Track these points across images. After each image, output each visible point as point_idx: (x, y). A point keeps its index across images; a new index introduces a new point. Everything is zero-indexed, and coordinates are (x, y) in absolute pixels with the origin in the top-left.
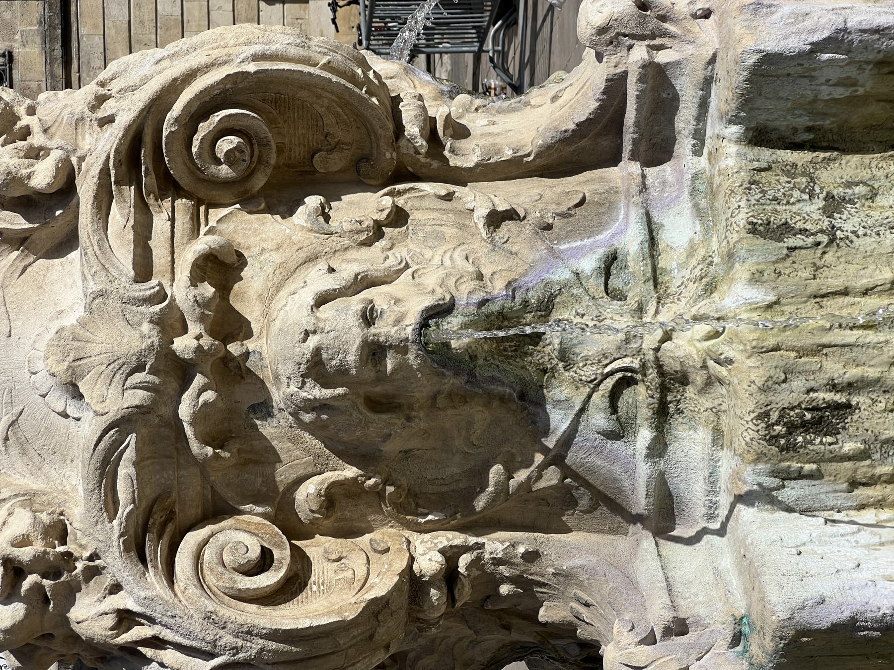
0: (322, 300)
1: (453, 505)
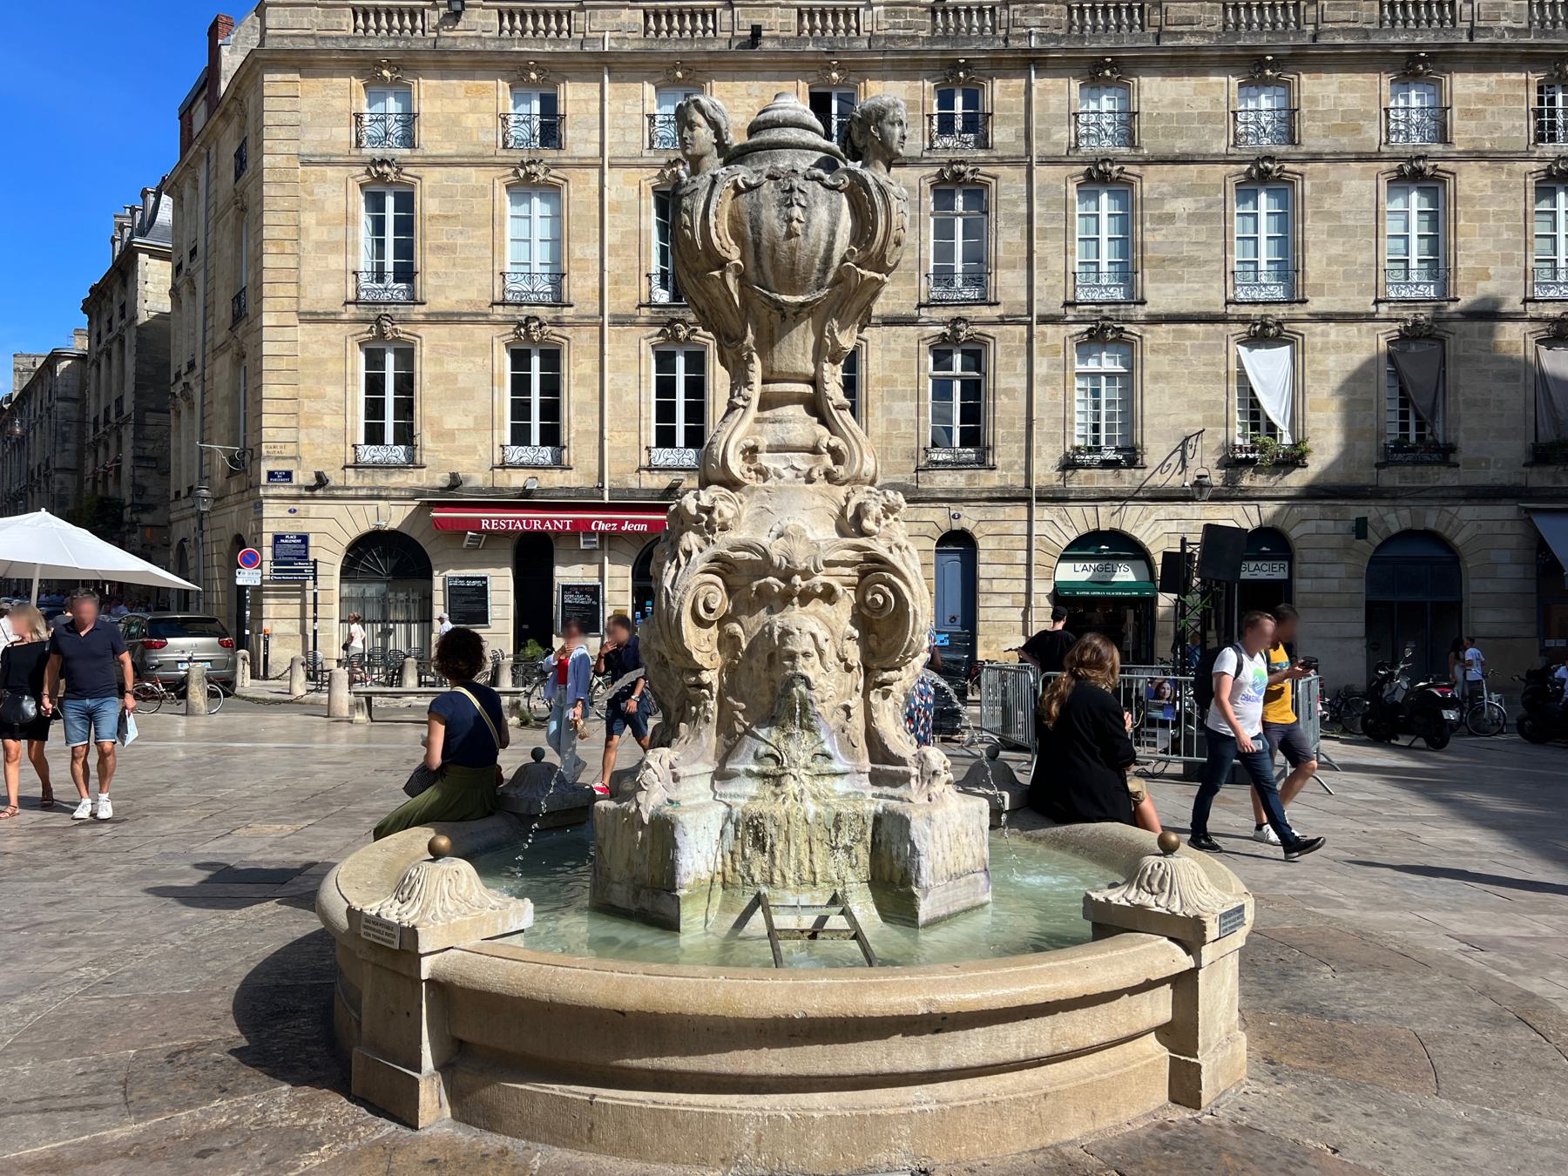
0: (813, 636)
1: (730, 688)
